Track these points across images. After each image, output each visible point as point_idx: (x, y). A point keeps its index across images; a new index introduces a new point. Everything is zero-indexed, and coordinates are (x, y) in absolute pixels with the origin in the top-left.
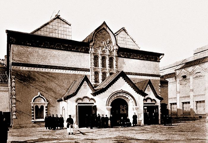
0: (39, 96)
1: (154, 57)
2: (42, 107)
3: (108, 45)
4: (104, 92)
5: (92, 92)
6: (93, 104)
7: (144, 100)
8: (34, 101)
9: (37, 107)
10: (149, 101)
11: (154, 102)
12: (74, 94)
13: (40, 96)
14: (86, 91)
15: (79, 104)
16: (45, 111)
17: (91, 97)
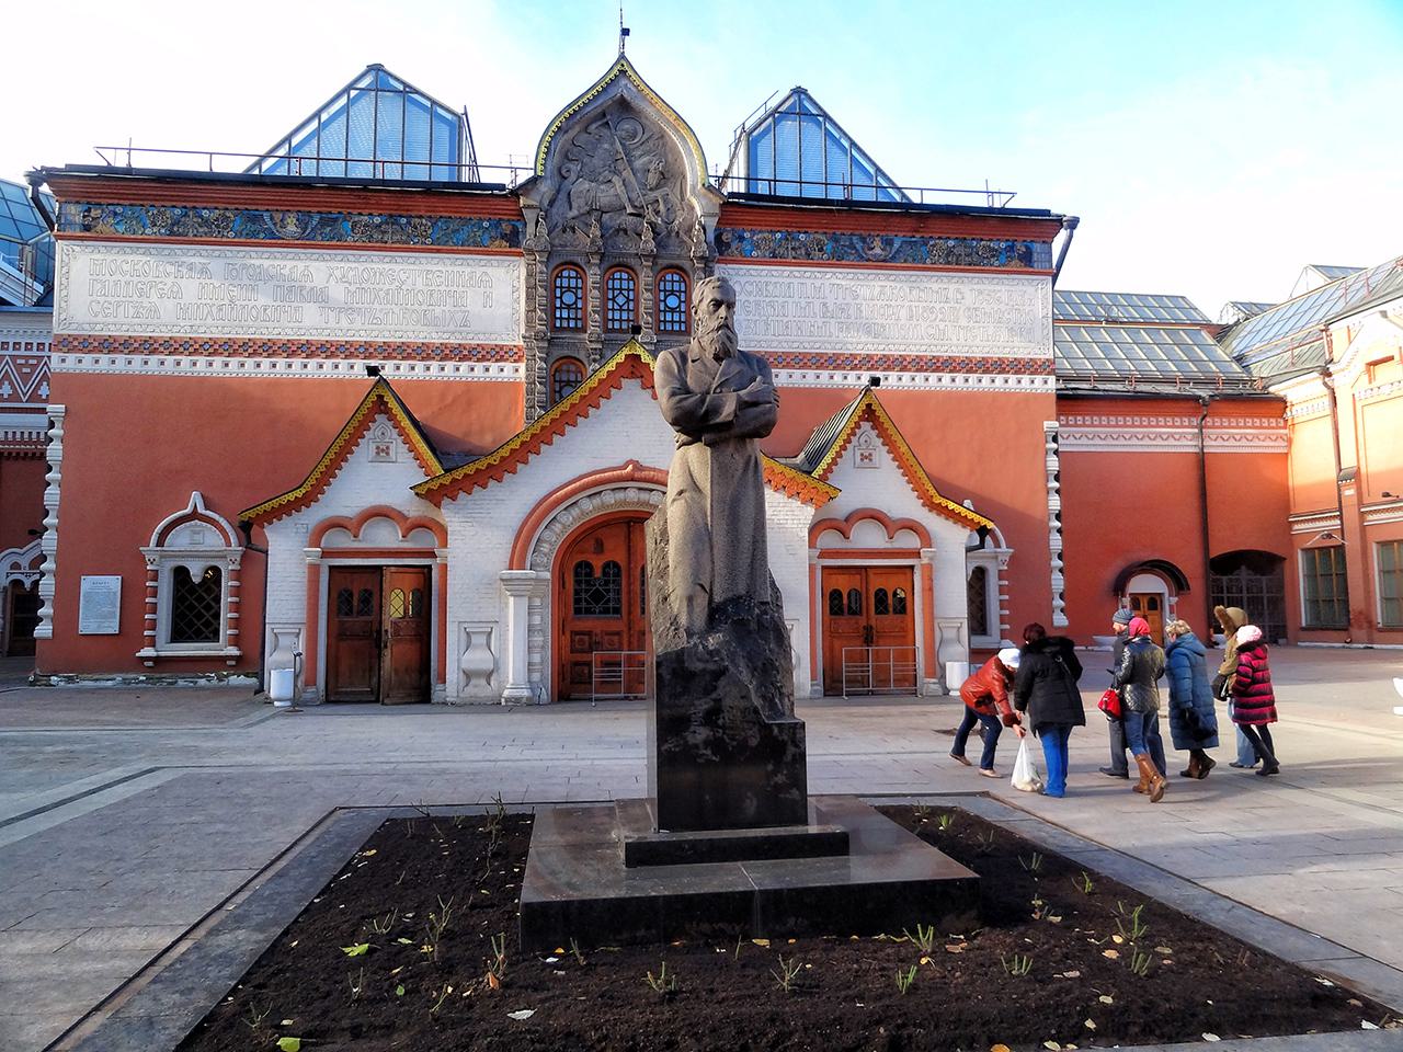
0: (194, 515)
1: (1013, 238)
2: (213, 578)
3: (653, 195)
4: (499, 480)
5: (420, 478)
6: (432, 555)
7: (815, 529)
8: (160, 543)
9: (181, 574)
10: (869, 537)
11: (910, 541)
12: (307, 500)
13: (201, 510)
14: (382, 478)
15: (325, 554)
16: (226, 599)
17: (415, 508)
